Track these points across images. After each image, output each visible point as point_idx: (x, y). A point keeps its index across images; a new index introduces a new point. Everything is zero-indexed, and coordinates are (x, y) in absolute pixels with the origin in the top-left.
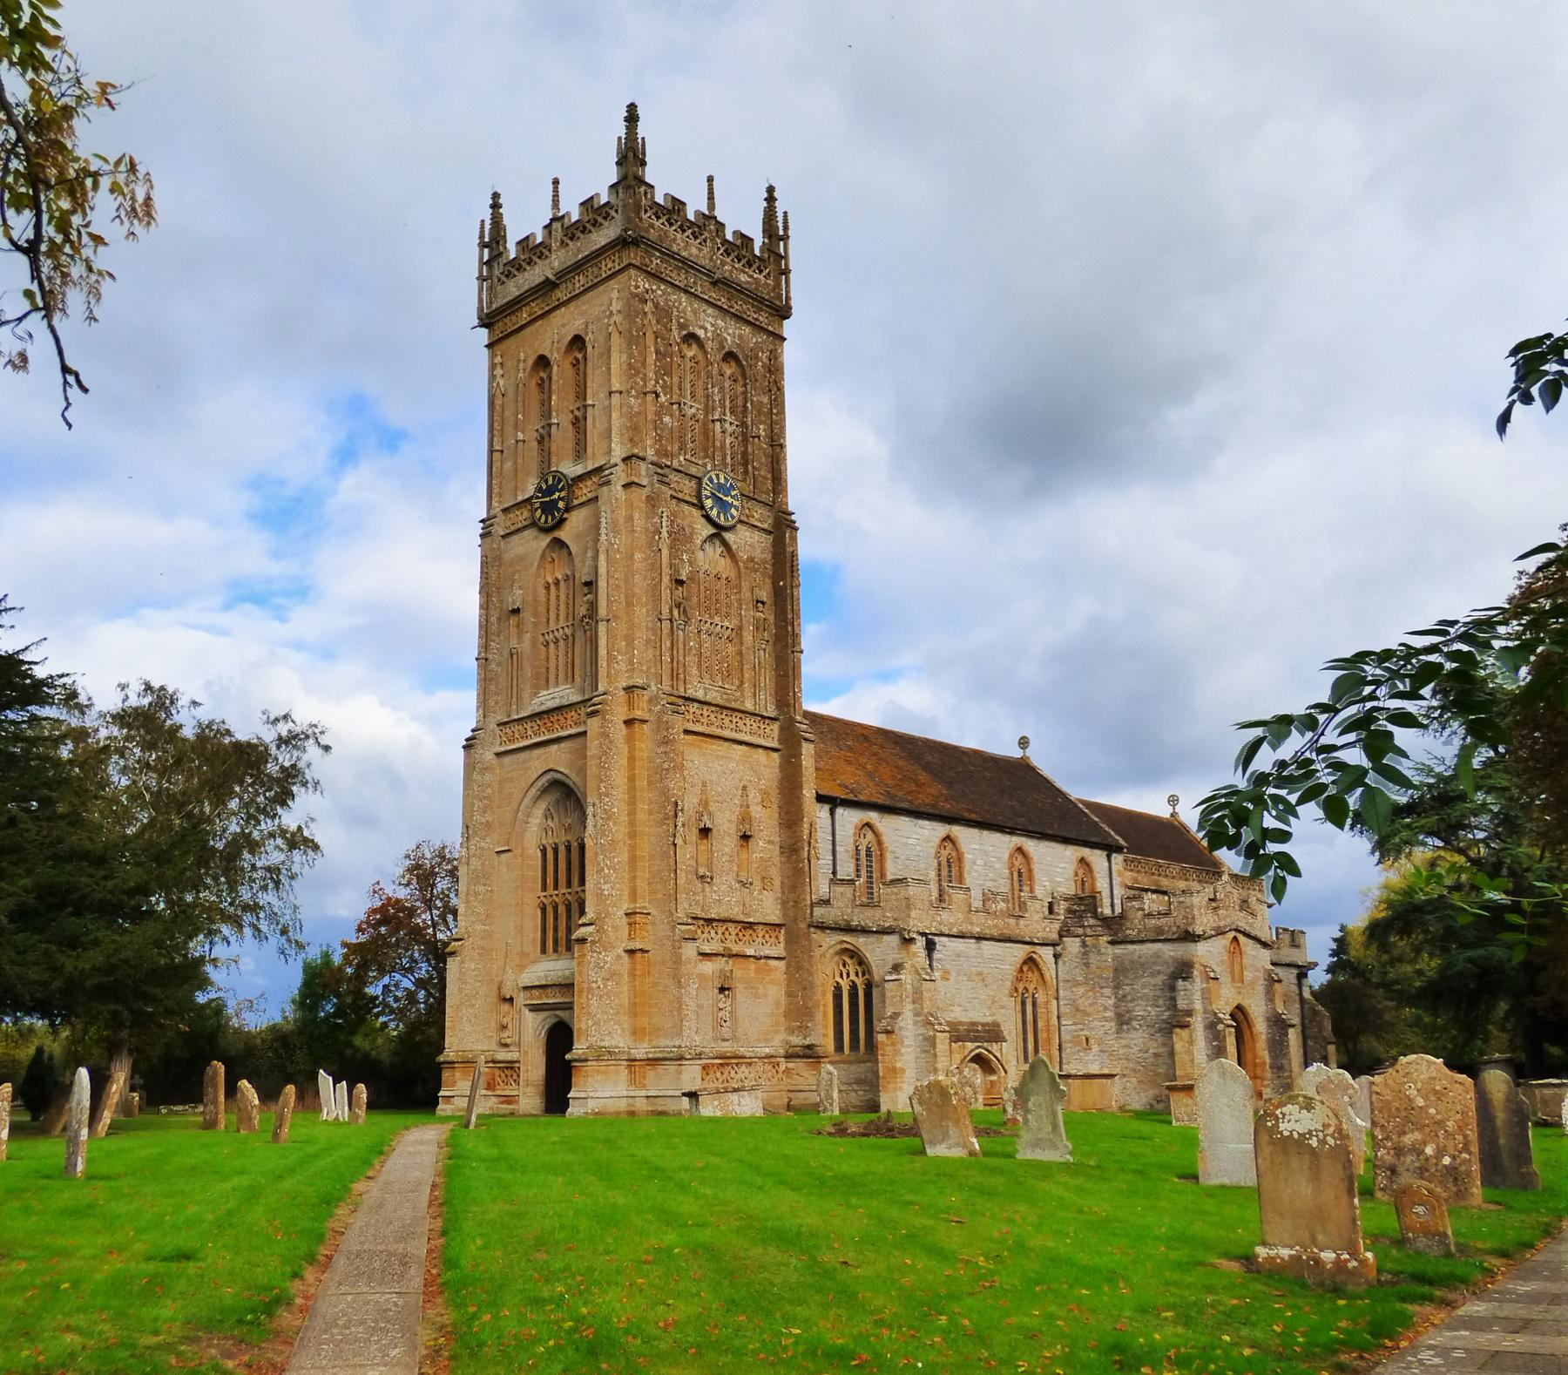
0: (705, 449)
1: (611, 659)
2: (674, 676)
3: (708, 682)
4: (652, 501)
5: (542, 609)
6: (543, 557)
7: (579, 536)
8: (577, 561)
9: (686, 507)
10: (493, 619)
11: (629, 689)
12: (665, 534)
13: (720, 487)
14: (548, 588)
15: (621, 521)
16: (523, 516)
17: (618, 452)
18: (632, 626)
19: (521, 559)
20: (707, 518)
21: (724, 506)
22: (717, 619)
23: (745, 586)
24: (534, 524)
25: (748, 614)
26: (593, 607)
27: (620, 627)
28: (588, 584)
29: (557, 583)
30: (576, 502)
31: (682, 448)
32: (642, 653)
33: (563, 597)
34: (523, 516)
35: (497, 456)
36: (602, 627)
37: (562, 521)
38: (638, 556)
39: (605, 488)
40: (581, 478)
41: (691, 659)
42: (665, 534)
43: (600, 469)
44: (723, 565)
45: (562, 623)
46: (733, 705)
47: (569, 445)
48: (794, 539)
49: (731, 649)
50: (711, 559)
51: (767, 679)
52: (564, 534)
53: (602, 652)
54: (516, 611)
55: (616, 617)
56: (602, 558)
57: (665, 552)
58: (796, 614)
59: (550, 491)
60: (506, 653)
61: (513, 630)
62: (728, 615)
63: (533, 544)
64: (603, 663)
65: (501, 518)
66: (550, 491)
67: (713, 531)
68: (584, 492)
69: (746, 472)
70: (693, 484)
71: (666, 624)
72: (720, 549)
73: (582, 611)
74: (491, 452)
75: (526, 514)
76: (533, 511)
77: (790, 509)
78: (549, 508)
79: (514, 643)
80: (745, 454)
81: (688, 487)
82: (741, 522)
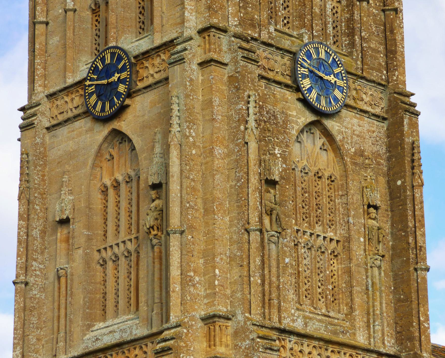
0: (301, 17)
1: (185, 281)
2: (266, 302)
3: (307, 307)
4: (236, 82)
5: (98, 219)
6: (99, 153)
7: (145, 127)
8: (142, 157)
9: (278, 91)
10: (36, 233)
11: (209, 319)
12: (252, 124)
13: (321, 63)
14: (105, 191)
15: (198, 108)
16: (74, 102)
17: (193, 21)
18: (211, 239)
19: (71, 155)
20: (305, 102)
21: (325, 87)
22: (318, 229)
23: (354, 187)
24: (87, 113)
25: (358, 221)
26: (163, 214)
27: (199, 242)
28: (156, 187)
29: (117, 185)
30: (140, 85)
31: (272, 15)
32: (225, 273)
33: (124, 204)
34: (74, 102)
35: (40, 28)
36: (175, 243)
37: (123, 108)
38: (219, 151)
39: (177, 68)
40: (146, 55)
41: (288, 280)
42: (252, 124)
43: (170, 44)
44: (325, 161)
45: (123, 236)
46: (341, 338)
47: (133, 14)
48: (414, 126)
49: (337, 266)
50: (309, 153)
51: (383, 305)
52: (124, 124)
53: (175, 272)
54: (65, 222)
55: (191, 227)
56: (174, 154)
57: (253, 146)
58: (419, 221)
59: (107, 72)
60: (52, 276)
61: (62, 246)
62: (332, 223)
63: (88, 136)
64: (176, 287)
65: (45, 106)
66: (107, 72)
67: (311, 118)
68: (150, 72)
69: (352, 44)
70: (287, 60)
71: (255, 236)
72: (320, 141)
73: (149, 220)
74: (33, 24)
75: (78, 101)
76: (86, 96)
77: (409, 88)
78: (105, 92)
79: (62, 262)
80: (350, 20)
81: (280, 64)
82: (347, 106)
